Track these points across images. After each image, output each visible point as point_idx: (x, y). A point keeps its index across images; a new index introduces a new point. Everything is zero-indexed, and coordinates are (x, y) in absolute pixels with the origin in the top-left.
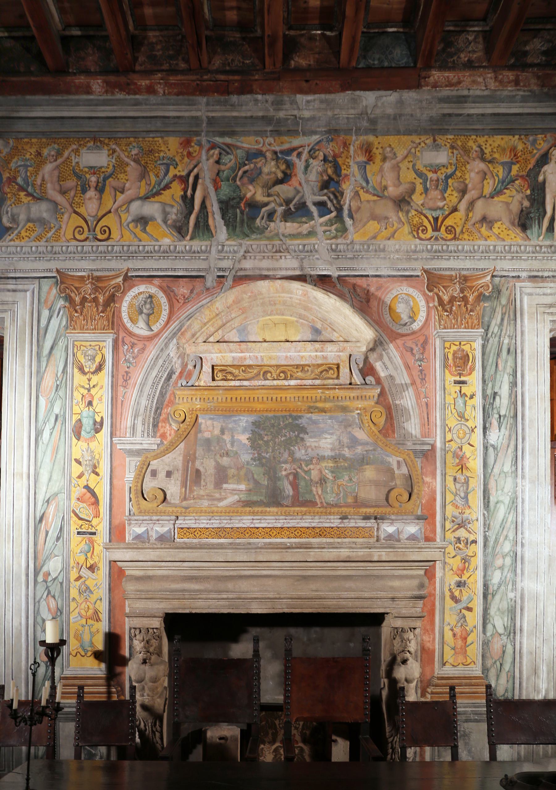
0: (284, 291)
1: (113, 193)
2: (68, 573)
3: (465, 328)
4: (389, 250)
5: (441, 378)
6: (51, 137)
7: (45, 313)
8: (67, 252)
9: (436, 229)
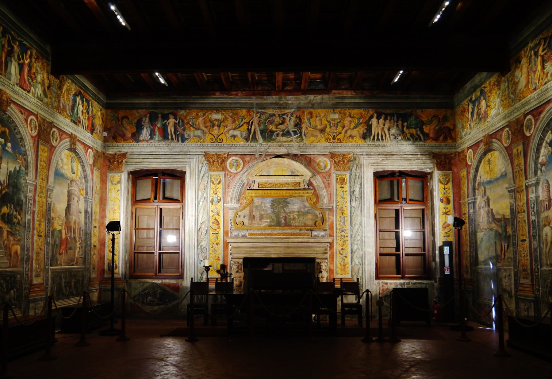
2: (209, 246)
5: (335, 186)
6: (202, 109)
7: (200, 165)
9: (334, 139)
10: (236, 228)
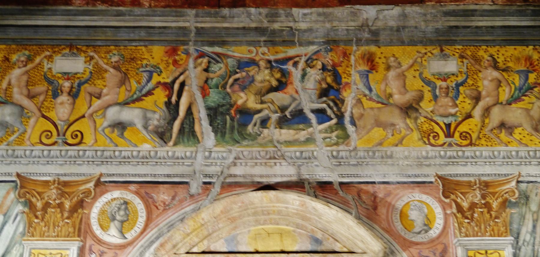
0: (278, 201)
1: (88, 98)
3: (491, 236)
4: (397, 156)
6: (22, 44)
8: (30, 156)
9: (449, 135)
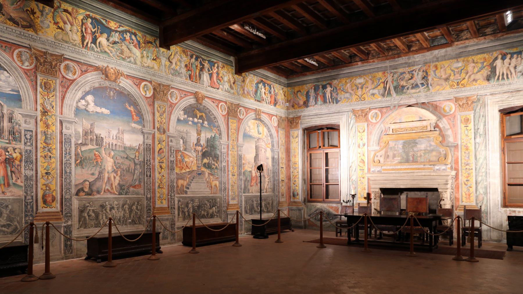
7: (350, 120)
9: (458, 85)
10: (374, 166)
